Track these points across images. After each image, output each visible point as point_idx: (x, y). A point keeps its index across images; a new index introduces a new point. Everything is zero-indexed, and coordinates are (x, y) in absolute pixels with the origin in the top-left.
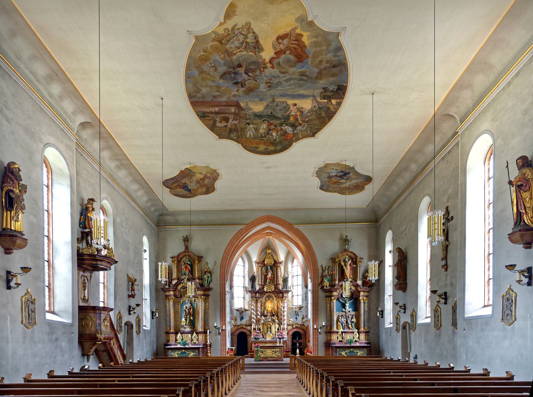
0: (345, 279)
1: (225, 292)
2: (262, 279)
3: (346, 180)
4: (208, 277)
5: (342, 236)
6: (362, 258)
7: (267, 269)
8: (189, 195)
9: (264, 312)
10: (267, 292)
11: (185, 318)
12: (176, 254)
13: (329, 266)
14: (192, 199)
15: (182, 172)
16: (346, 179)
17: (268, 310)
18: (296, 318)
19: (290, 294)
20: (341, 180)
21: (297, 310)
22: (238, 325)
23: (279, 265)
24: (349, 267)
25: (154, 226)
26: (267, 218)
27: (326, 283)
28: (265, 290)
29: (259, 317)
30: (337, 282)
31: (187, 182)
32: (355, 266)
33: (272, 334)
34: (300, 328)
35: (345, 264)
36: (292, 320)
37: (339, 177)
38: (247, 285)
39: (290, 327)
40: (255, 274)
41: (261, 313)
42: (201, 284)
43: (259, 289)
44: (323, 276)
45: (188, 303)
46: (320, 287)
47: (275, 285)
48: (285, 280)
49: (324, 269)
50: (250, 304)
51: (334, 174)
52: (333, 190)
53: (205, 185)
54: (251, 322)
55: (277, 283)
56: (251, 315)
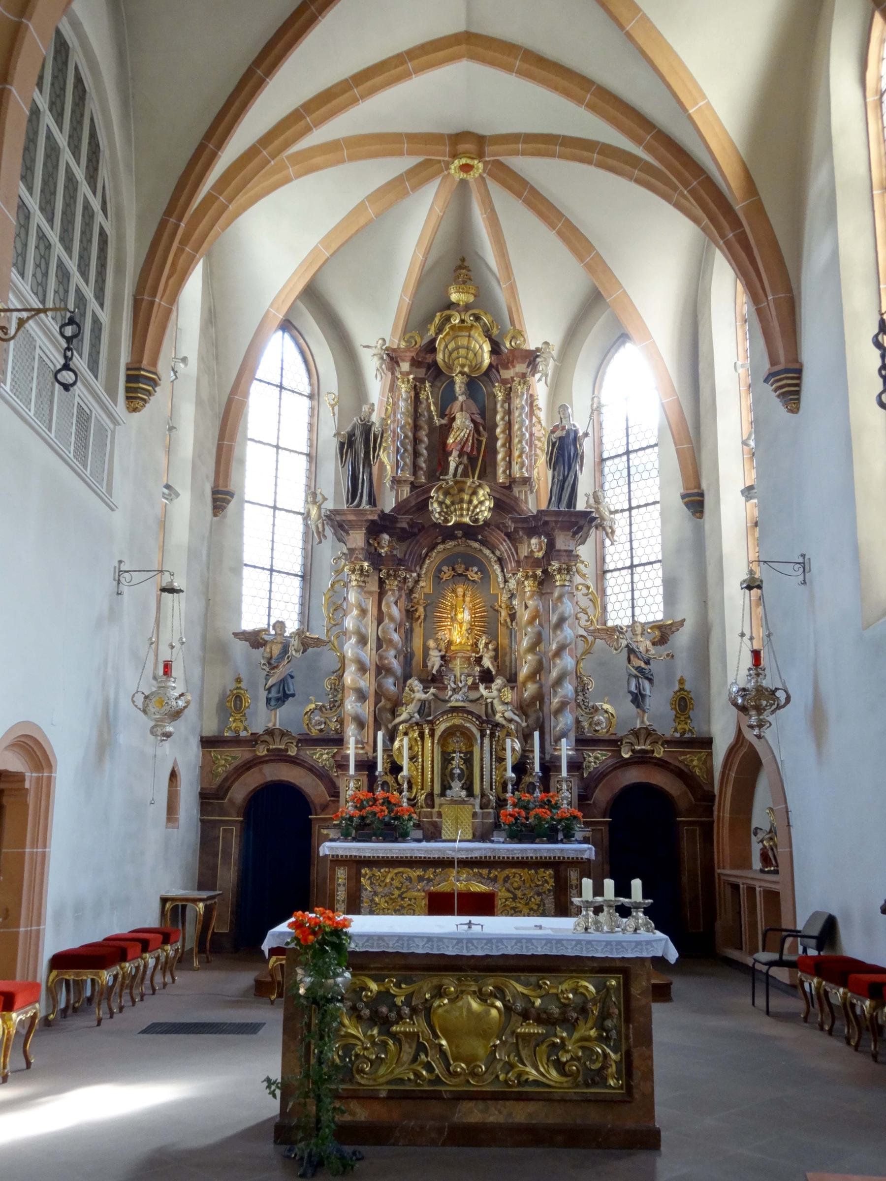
2: (416, 454)
7: (447, 399)
9: (426, 649)
10: (448, 534)
17: (450, 643)
18: (638, 699)
22: (254, 740)
23: (520, 368)
28: (436, 517)
29: (389, 683)
33: (478, 801)
34: (662, 764)
39: (596, 758)
40: (375, 418)
41: (407, 658)
43: (401, 507)
54: (341, 722)
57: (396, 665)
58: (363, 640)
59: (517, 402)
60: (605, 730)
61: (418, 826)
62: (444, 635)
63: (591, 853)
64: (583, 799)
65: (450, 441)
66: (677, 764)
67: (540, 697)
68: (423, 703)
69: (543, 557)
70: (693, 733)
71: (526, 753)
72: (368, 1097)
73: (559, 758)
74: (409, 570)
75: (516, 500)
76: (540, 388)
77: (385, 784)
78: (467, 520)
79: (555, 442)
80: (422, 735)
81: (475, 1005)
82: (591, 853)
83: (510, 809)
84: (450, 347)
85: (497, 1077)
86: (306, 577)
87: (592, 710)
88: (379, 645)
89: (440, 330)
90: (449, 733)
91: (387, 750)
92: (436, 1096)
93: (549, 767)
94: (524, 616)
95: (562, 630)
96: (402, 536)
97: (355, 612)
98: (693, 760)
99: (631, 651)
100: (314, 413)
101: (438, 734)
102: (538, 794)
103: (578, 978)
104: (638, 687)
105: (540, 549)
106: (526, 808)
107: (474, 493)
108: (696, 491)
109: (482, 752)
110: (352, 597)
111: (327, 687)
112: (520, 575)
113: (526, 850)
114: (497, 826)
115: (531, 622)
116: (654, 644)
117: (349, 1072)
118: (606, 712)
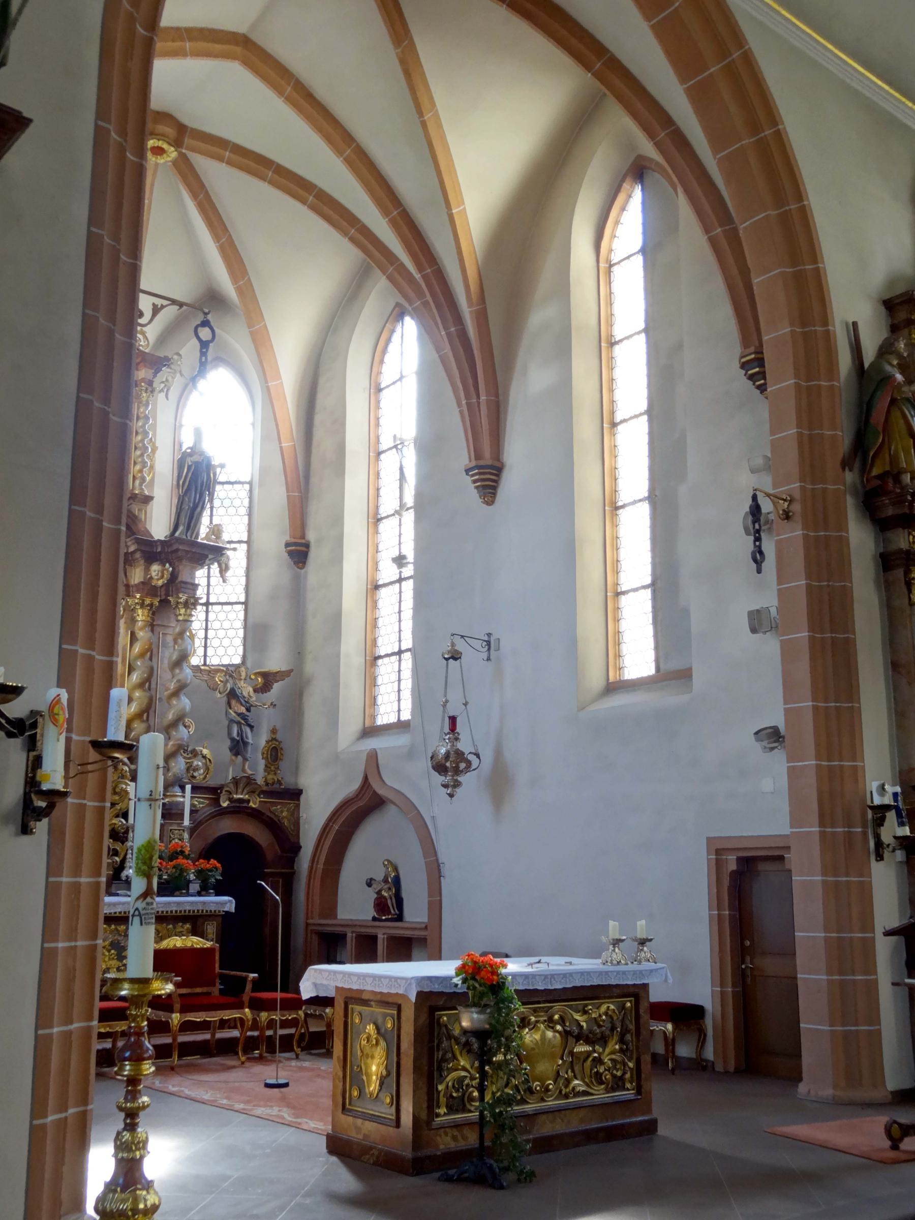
34: (255, 815)
60: (202, 777)
63: (231, 906)
66: (269, 814)
69: (162, 586)
70: (281, 784)
79: (191, 465)
82: (231, 906)
85: (561, 1091)
87: (190, 755)
95: (181, 669)
98: (282, 812)
99: (233, 695)
103: (608, 1003)
104: (240, 733)
105: (162, 577)
108: (303, 541)
113: (169, 903)
116: (255, 691)
118: (204, 757)
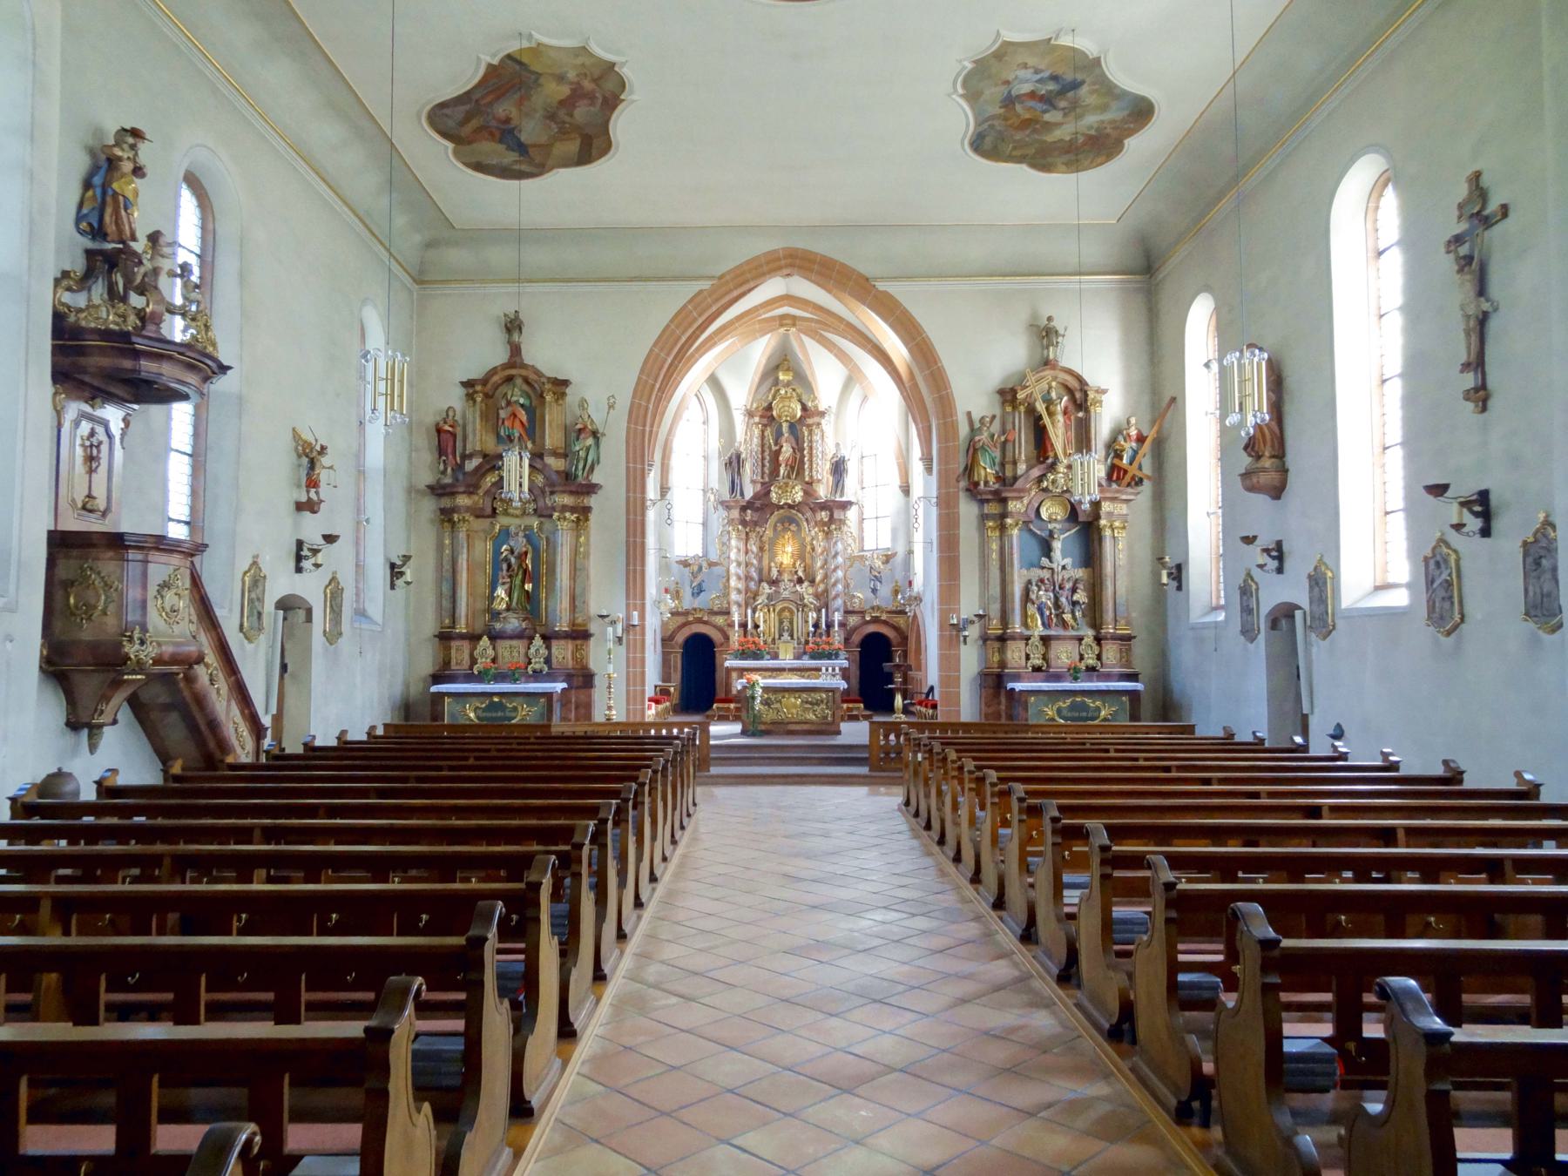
0: (1047, 458)
1: (643, 500)
2: (763, 466)
3: (1065, 115)
4: (588, 449)
5: (1035, 315)
6: (1104, 392)
7: (779, 434)
8: (524, 168)
9: (770, 568)
10: (780, 507)
11: (507, 586)
12: (476, 373)
13: (994, 417)
14: (527, 183)
15: (492, 71)
16: (1063, 109)
17: (782, 563)
18: (874, 591)
19: (852, 514)
20: (1045, 112)
21: (878, 563)
22: (686, 613)
23: (816, 419)
24: (1060, 418)
25: (408, 281)
26: (785, 258)
27: (987, 471)
29: (752, 585)
30: (1022, 468)
31: (514, 113)
32: (1081, 414)
34: (885, 623)
35: (1047, 408)
36: (861, 596)
37: (1042, 99)
38: (714, 484)
39: (853, 620)
40: (742, 449)
41: (760, 571)
42: (563, 472)
43: (756, 496)
44: (975, 450)
45: (517, 534)
46: (963, 484)
47: (807, 483)
48: (838, 468)
49: (977, 425)
50: (724, 544)
51: (1026, 88)
52: (1014, 153)
53: (577, 128)
54: (729, 603)
55: (811, 477)
56: (728, 580)
57: (755, 575)
58: (739, 564)
59: (815, 438)
61: (768, 653)
62: (779, 559)
64: (847, 640)
65: (781, 458)
67: (826, 591)
68: (769, 594)
71: (819, 618)
72: (765, 723)
73: (834, 621)
74: (761, 527)
75: (815, 491)
76: (827, 424)
77: (752, 634)
78: (790, 501)
80: (769, 611)
81: (793, 700)
83: (811, 645)
84: (781, 406)
86: (705, 524)
88: (747, 566)
89: (774, 398)
90: (783, 610)
91: (753, 618)
92: (782, 723)
93: (829, 625)
94: (819, 550)
96: (756, 510)
97: (735, 550)
98: (900, 621)
100: (706, 432)
101: (777, 611)
102: (824, 638)
106: (818, 645)
107: (793, 488)
109: (798, 619)
110: (733, 542)
111: (721, 586)
112: (816, 529)
114: (805, 653)
115: (822, 553)
117: (760, 717)
